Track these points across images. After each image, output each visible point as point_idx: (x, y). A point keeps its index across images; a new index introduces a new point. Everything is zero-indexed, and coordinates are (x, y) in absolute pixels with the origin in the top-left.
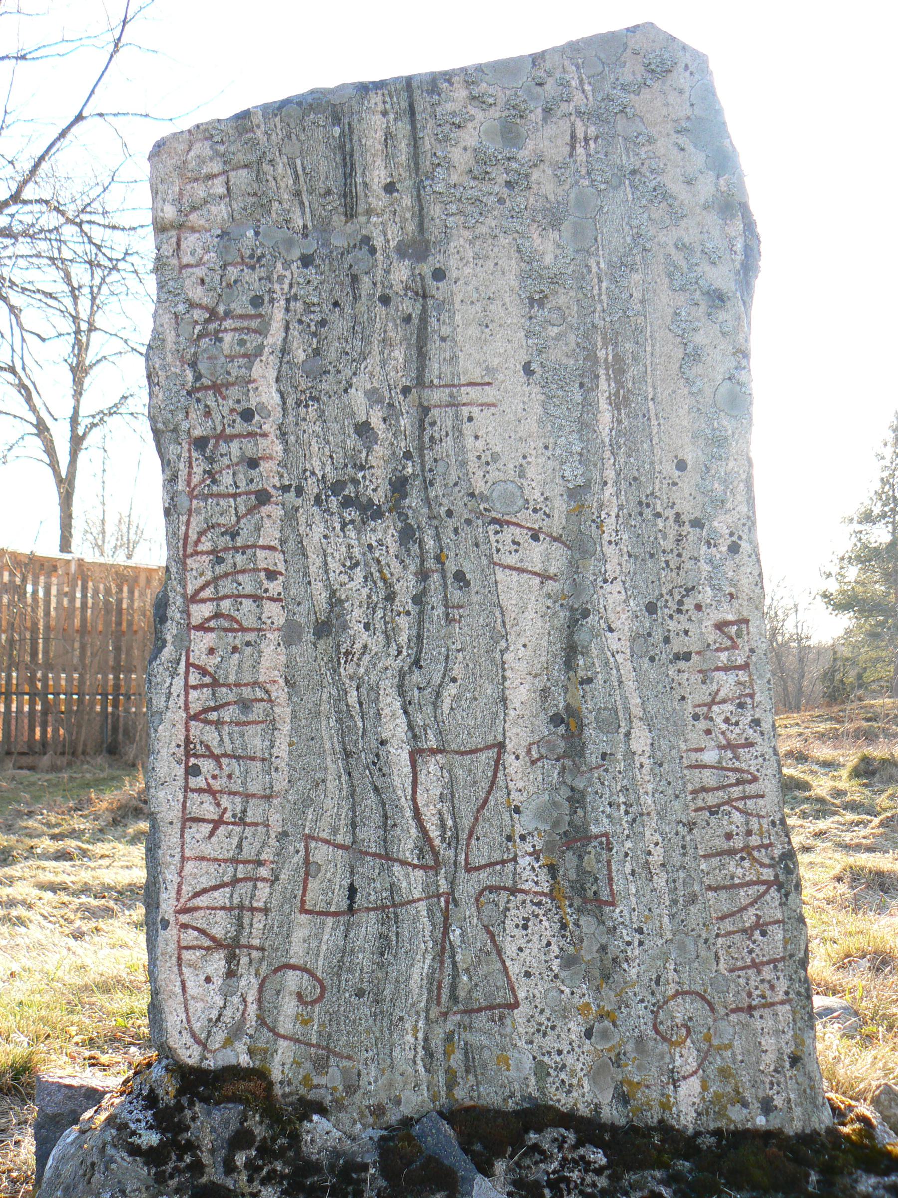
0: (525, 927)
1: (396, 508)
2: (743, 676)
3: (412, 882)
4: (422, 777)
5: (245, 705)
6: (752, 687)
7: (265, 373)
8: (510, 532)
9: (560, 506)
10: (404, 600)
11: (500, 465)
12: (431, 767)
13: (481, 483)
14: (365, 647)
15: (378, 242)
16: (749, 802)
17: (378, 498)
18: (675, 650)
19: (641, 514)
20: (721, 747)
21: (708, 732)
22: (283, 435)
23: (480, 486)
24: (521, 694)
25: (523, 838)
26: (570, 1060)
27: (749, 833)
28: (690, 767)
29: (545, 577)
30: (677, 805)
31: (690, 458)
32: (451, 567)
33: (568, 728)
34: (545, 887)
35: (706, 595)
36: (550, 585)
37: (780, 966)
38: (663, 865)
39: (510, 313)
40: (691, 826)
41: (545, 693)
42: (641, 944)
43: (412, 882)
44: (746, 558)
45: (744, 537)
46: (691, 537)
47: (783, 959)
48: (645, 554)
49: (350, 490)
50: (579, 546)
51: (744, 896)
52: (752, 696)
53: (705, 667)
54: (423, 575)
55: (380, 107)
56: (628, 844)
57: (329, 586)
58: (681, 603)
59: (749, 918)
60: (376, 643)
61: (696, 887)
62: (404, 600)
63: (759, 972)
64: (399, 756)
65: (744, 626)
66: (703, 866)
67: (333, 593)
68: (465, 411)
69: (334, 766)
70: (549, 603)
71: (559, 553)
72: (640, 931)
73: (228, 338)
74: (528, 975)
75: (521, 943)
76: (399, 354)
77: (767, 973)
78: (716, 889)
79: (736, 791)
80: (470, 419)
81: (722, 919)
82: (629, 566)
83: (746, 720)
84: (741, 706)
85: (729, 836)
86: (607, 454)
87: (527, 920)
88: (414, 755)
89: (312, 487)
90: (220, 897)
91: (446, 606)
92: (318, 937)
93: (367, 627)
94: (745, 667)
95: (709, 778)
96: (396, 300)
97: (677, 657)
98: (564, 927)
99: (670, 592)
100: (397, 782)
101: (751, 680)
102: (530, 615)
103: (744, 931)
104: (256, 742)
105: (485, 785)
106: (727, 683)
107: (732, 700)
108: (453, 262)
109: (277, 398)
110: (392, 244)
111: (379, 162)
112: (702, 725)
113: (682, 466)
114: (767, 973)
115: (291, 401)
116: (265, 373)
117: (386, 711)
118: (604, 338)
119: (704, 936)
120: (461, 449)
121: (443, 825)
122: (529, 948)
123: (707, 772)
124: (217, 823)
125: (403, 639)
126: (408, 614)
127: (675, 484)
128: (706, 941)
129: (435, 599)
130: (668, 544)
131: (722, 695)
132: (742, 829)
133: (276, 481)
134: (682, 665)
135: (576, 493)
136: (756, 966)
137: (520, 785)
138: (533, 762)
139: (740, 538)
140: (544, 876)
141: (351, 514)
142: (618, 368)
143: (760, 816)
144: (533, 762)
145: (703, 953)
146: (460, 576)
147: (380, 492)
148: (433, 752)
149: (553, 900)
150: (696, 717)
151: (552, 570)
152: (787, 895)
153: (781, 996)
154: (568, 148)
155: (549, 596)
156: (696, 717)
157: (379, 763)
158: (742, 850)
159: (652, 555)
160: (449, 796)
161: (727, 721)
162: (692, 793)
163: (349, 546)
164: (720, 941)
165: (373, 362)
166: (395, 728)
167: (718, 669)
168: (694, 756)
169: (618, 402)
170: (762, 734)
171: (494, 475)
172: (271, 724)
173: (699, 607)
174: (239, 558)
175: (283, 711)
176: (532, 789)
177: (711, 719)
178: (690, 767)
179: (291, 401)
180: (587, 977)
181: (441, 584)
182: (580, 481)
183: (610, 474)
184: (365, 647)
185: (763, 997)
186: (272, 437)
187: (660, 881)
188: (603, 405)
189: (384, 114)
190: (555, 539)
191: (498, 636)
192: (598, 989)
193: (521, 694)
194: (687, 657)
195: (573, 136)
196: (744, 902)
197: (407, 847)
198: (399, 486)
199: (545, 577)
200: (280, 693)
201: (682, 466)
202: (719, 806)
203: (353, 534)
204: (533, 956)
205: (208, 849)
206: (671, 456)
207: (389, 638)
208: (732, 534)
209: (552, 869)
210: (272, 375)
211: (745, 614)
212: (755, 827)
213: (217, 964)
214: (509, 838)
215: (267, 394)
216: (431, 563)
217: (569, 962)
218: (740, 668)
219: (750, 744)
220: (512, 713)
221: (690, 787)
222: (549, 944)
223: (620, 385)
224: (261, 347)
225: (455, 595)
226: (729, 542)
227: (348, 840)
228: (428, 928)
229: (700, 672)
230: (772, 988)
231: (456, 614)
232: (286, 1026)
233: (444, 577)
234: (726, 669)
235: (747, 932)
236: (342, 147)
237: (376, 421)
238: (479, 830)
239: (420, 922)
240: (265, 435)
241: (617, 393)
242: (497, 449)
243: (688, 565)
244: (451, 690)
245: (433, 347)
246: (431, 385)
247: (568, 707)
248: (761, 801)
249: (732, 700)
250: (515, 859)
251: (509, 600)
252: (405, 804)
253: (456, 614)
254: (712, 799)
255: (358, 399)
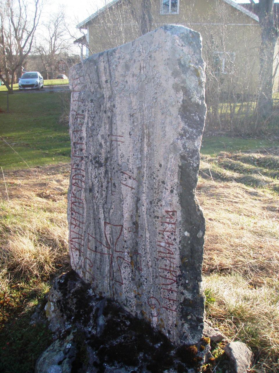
0: (125, 268)
1: (105, 165)
2: (173, 226)
3: (105, 250)
4: (106, 228)
5: (79, 203)
6: (175, 230)
7: (84, 129)
8: (125, 176)
9: (135, 171)
10: (104, 187)
11: (124, 158)
12: (108, 227)
13: (120, 162)
14: (97, 196)
15: (105, 96)
16: (171, 259)
17: (103, 161)
18: (155, 215)
19: (151, 177)
20: (166, 243)
21: (163, 238)
22: (86, 144)
23: (120, 163)
24: (126, 215)
25: (126, 248)
26: (132, 301)
27: (171, 267)
28: (158, 245)
29: (132, 188)
30: (155, 253)
31: (163, 164)
32: (113, 182)
33: (136, 226)
34: (130, 261)
35: (163, 203)
36: (133, 191)
37: (175, 302)
38: (151, 266)
39: (126, 118)
40: (158, 259)
41: (132, 216)
42: (146, 282)
43: (105, 250)
44: (175, 195)
45: (175, 189)
46: (161, 186)
47: (176, 301)
48: (151, 188)
49: (97, 159)
50: (140, 183)
51: (168, 282)
52: (175, 232)
53: (163, 221)
54: (108, 182)
55: (102, 61)
56: (144, 258)
57: (92, 181)
58: (157, 203)
59: (169, 287)
60: (99, 196)
61: (158, 275)
62: (104, 187)
63: (170, 301)
64: (102, 222)
65: (175, 213)
66: (159, 270)
67: (93, 183)
68: (118, 143)
69: (92, 221)
70: (133, 195)
71: (135, 182)
72: (146, 279)
73: (79, 119)
74: (125, 279)
75: (124, 271)
76: (107, 126)
77: (171, 302)
78: (162, 277)
79: (168, 255)
80: (119, 145)
81: (163, 284)
82: (147, 191)
83: (173, 238)
84: (172, 234)
85: (166, 266)
86: (145, 159)
87: (125, 267)
88: (105, 223)
89: (90, 158)
90: (76, 240)
91: (112, 191)
92: (91, 254)
93: (98, 192)
94: (174, 224)
95: (162, 249)
96: (107, 112)
97: (155, 217)
98: (132, 271)
99: (155, 199)
100: (102, 228)
101: (175, 228)
102: (128, 197)
103: (168, 290)
104: (81, 212)
105: (119, 234)
106: (169, 227)
107: (170, 232)
108: (116, 103)
109: (86, 135)
110: (108, 97)
111: (104, 75)
112: (161, 236)
113: (160, 166)
114: (171, 302)
115: (88, 136)
116: (84, 129)
117: (100, 212)
118: (146, 127)
119: (159, 287)
120: (118, 153)
121: (110, 240)
122: (126, 273)
123: (162, 248)
124: (76, 226)
125: (104, 196)
126: (105, 191)
127: (159, 171)
128: (159, 288)
129: (110, 189)
130: (156, 187)
131: (167, 229)
132: (169, 265)
133: (85, 155)
134: (156, 219)
135: (139, 168)
136: (170, 300)
137: (126, 236)
138: (129, 232)
139: (174, 189)
140: (129, 258)
141: (97, 165)
142: (149, 137)
143: (174, 264)
144: (129, 232)
145: (158, 291)
146: (114, 184)
147: (103, 160)
148: (109, 224)
149: (131, 264)
150: (159, 233)
151: (134, 187)
152: (179, 285)
153: (174, 309)
154: (139, 70)
155: (133, 193)
156: (159, 233)
157: (99, 223)
158: (169, 270)
159: (152, 189)
160: (111, 234)
161: (168, 237)
162: (158, 252)
163: (96, 173)
164: (162, 290)
165: (102, 128)
166: (102, 216)
167: (166, 223)
168: (159, 243)
169: (149, 145)
170: (176, 243)
171: (123, 160)
172: (83, 208)
173: (161, 205)
174: (79, 171)
175: (85, 206)
176: (129, 238)
177: (164, 235)
178: (158, 245)
179: (88, 136)
180: (136, 284)
181: (111, 186)
182: (140, 166)
183: (146, 165)
184: (97, 196)
185: (170, 307)
186: (84, 145)
187: (151, 269)
188: (145, 146)
189: (104, 62)
190: (134, 179)
191: (121, 201)
192: (138, 288)
193: (126, 215)
194: (158, 217)
195: (140, 67)
196: (168, 283)
197: (104, 242)
198: (107, 159)
199: (132, 188)
200: (84, 202)
201: (160, 166)
202: (164, 257)
203: (96, 170)
204: (126, 274)
205: (74, 230)
206: (158, 163)
207: (102, 195)
208: (172, 187)
209: (131, 257)
210: (85, 130)
211: (175, 210)
212: (172, 266)
213: (78, 253)
214: (124, 247)
215: (84, 134)
216: (109, 180)
217: (133, 279)
218: (173, 224)
219: (173, 245)
220: (124, 219)
221: (157, 250)
222: (129, 274)
223: (149, 141)
224: (84, 122)
225: (113, 189)
226: (171, 189)
227: (95, 237)
228: (108, 261)
229: (161, 222)
230: (172, 306)
231: (113, 193)
232: (88, 270)
233: (111, 184)
234: (168, 223)
235: (169, 290)
236: (97, 71)
237: (103, 143)
238: (118, 243)
239: (107, 258)
240: (83, 144)
241: (148, 143)
242: (124, 154)
243: (160, 193)
244: (112, 211)
245: (113, 125)
246: (113, 135)
247: (136, 221)
248: (174, 260)
249: (170, 232)
250: (124, 252)
251: (124, 192)
252: (103, 233)
253: (113, 193)
254: (163, 255)
255: (99, 137)
